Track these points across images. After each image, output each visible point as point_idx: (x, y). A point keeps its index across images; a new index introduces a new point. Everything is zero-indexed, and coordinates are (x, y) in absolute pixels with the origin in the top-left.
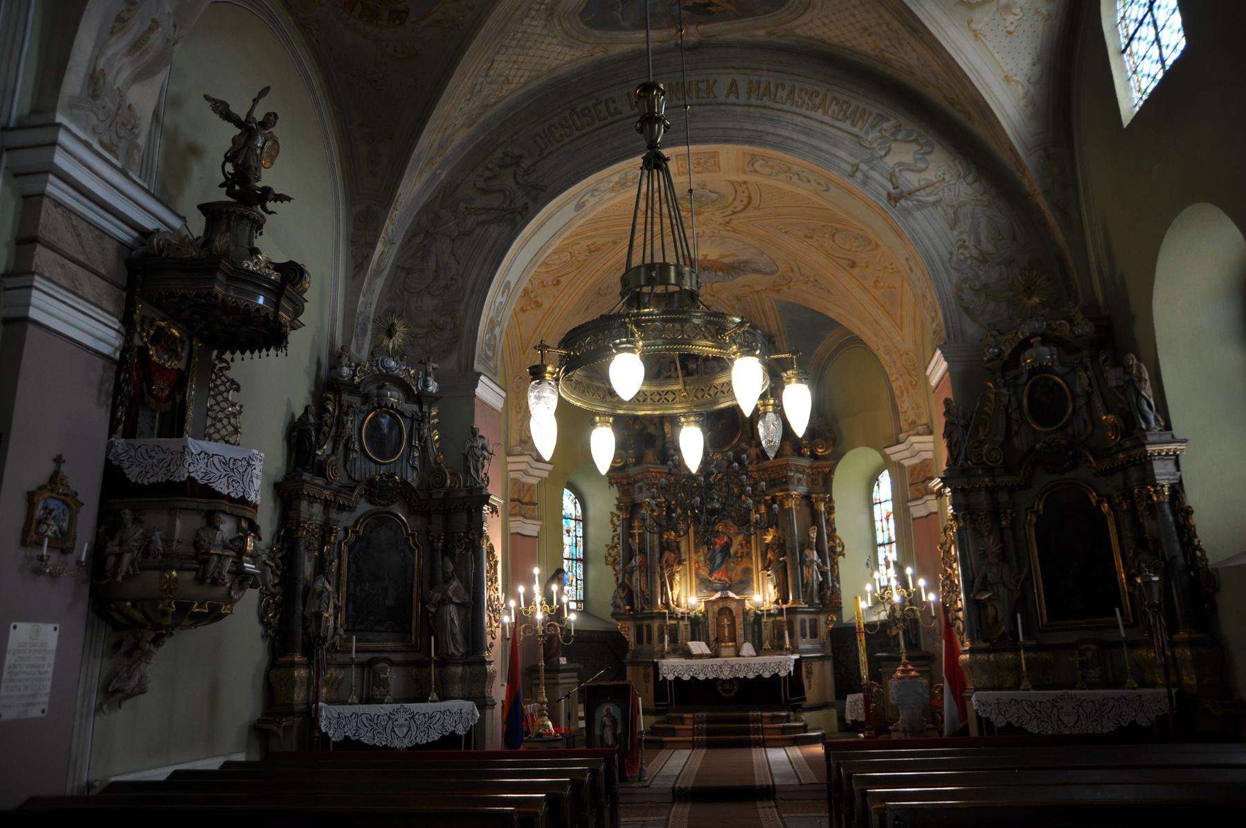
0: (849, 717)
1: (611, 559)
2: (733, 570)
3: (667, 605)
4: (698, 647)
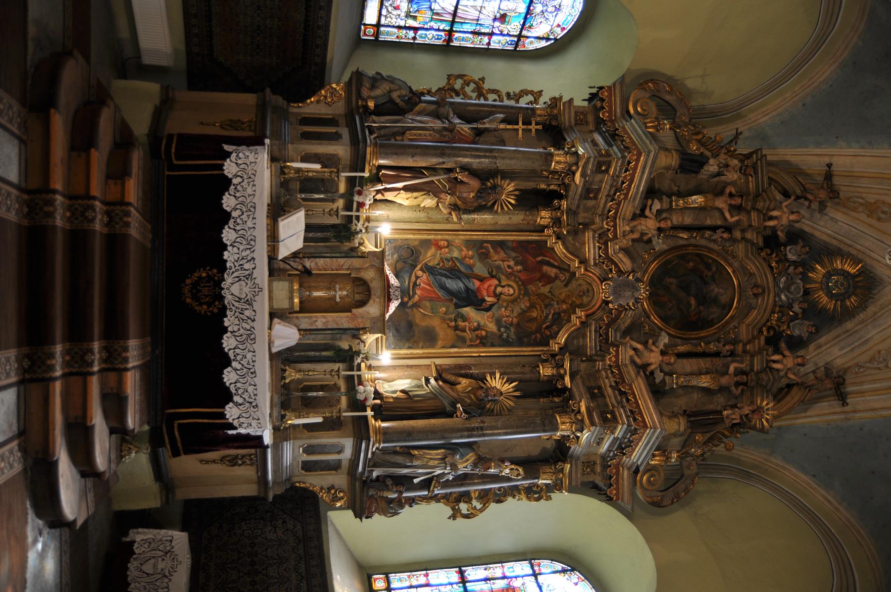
0: (140, 536)
2: (433, 310)
3: (376, 179)
4: (293, 231)
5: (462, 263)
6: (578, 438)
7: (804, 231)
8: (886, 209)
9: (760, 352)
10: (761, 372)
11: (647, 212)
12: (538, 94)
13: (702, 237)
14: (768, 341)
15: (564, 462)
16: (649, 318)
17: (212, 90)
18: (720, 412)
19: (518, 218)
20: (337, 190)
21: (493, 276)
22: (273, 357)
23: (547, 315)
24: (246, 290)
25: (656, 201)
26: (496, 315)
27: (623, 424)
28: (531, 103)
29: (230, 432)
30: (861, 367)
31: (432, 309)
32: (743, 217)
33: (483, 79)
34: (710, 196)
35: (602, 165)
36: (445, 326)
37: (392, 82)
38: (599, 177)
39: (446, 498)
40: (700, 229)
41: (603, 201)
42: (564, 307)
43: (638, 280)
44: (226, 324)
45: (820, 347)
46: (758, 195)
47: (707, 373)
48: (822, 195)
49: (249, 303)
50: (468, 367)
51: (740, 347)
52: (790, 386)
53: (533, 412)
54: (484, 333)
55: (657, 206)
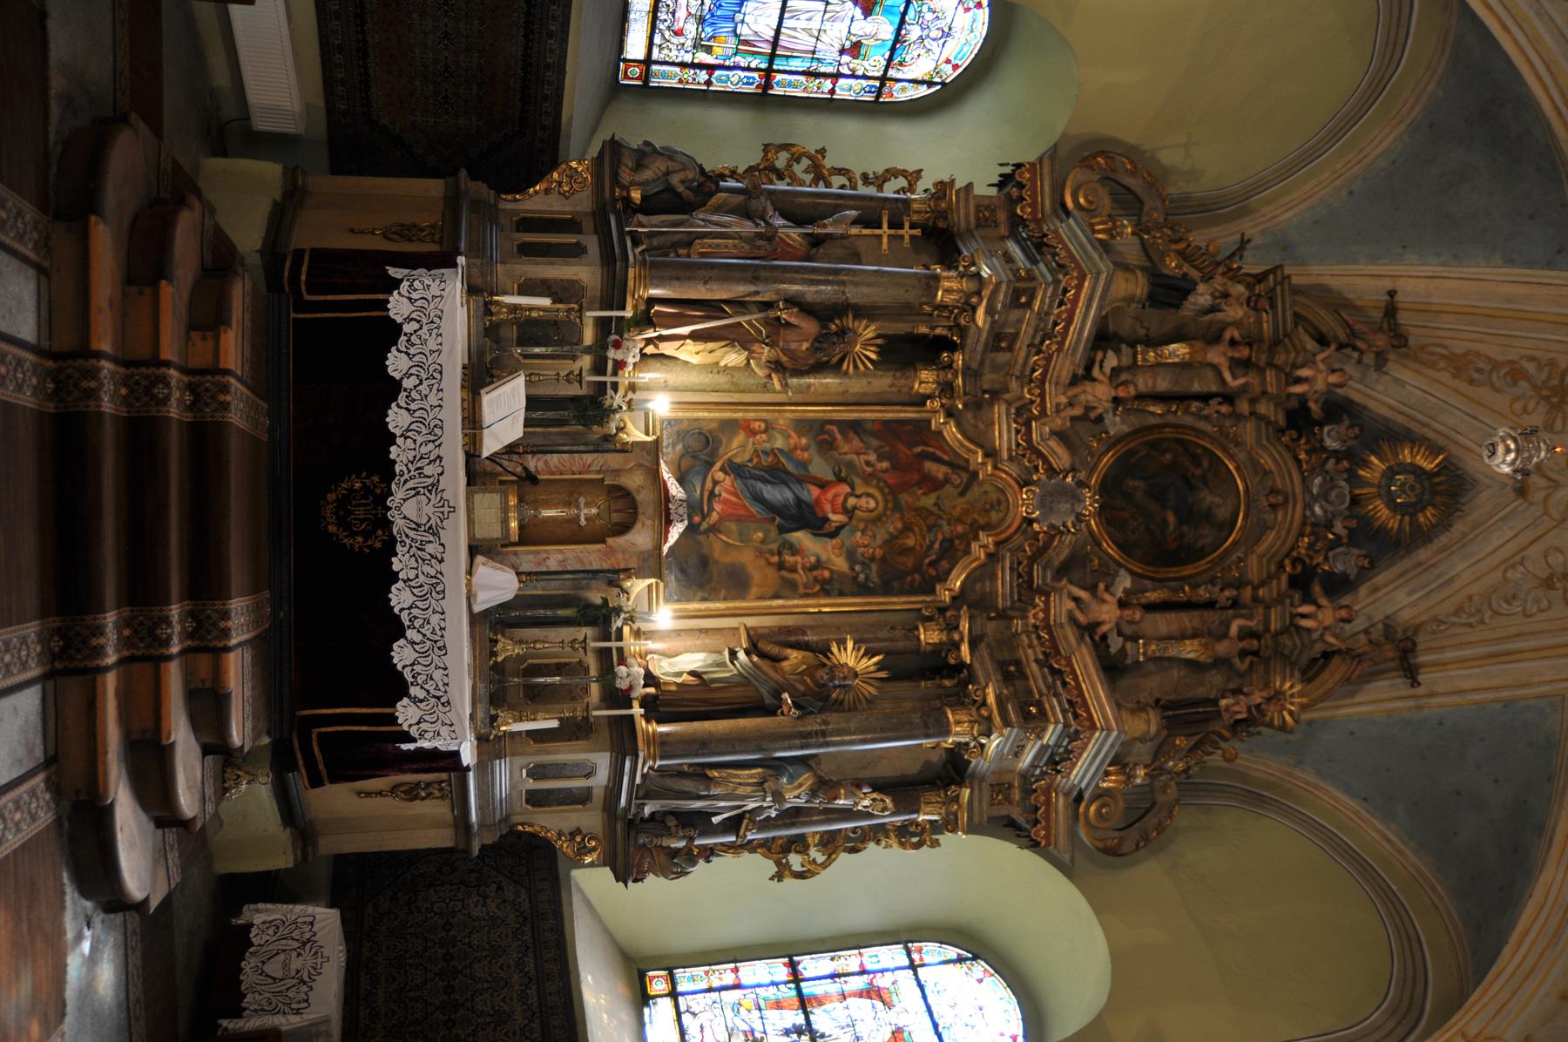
0: (261, 916)
1: (781, 160)
2: (744, 538)
3: (645, 320)
4: (506, 412)
5: (790, 458)
6: (982, 746)
7: (1351, 401)
8: (1481, 365)
9: (1279, 600)
10: (1282, 633)
11: (1096, 372)
12: (914, 177)
13: (1186, 411)
14: (1294, 582)
15: (960, 784)
16: (1099, 545)
17: (372, 174)
18: (1215, 702)
19: (883, 383)
20: (581, 340)
21: (841, 480)
22: (475, 619)
23: (932, 543)
24: (429, 510)
25: (1110, 353)
26: (848, 544)
27: (1057, 722)
28: (903, 190)
29: (405, 747)
30: (1442, 622)
31: (741, 534)
32: (1252, 379)
33: (822, 152)
34: (1198, 345)
35: (1020, 295)
36: (762, 562)
37: (671, 158)
38: (1015, 314)
39: (766, 847)
40: (1183, 398)
41: (1023, 354)
42: (960, 529)
43: (1081, 484)
44: (395, 568)
45: (1376, 590)
46: (1276, 343)
47: (1193, 636)
48: (1381, 341)
49: (434, 531)
50: (800, 630)
51: (1247, 593)
52: (1327, 656)
53: (908, 705)
54: (827, 574)
55: (1112, 361)
